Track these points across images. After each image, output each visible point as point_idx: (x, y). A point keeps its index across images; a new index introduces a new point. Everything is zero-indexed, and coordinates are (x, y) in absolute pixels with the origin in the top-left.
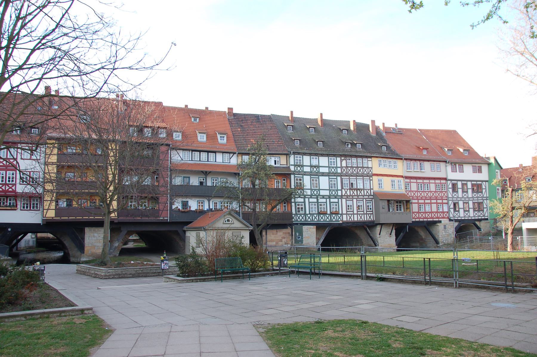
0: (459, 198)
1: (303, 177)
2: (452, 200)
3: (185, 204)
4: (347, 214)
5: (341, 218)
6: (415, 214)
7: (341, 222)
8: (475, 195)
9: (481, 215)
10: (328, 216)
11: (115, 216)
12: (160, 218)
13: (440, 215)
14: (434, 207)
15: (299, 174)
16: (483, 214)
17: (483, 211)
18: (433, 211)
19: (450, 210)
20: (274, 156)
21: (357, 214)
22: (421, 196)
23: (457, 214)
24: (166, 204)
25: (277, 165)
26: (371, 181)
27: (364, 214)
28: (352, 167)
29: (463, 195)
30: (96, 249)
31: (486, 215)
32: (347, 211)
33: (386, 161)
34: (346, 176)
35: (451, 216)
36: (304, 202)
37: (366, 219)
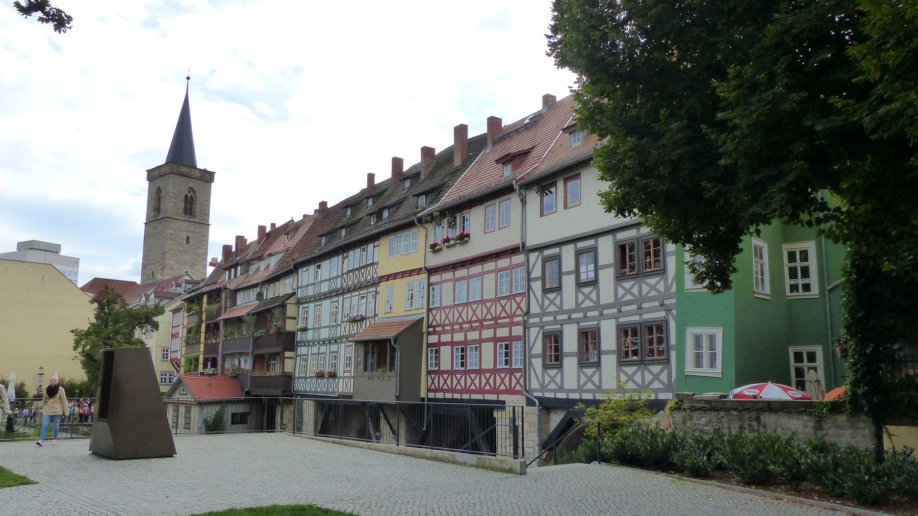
0: (565, 312)
1: (308, 307)
2: (541, 326)
4: (344, 377)
6: (445, 376)
8: (628, 291)
9: (656, 385)
10: (325, 380)
13: (503, 382)
14: (487, 357)
15: (306, 302)
16: (664, 377)
18: (483, 367)
19: (530, 363)
22: (460, 320)
23: (552, 379)
25: (291, 291)
26: (377, 295)
28: (354, 270)
29: (581, 297)
32: (345, 372)
33: (400, 236)
34: (349, 291)
35: (535, 384)
36: (307, 355)
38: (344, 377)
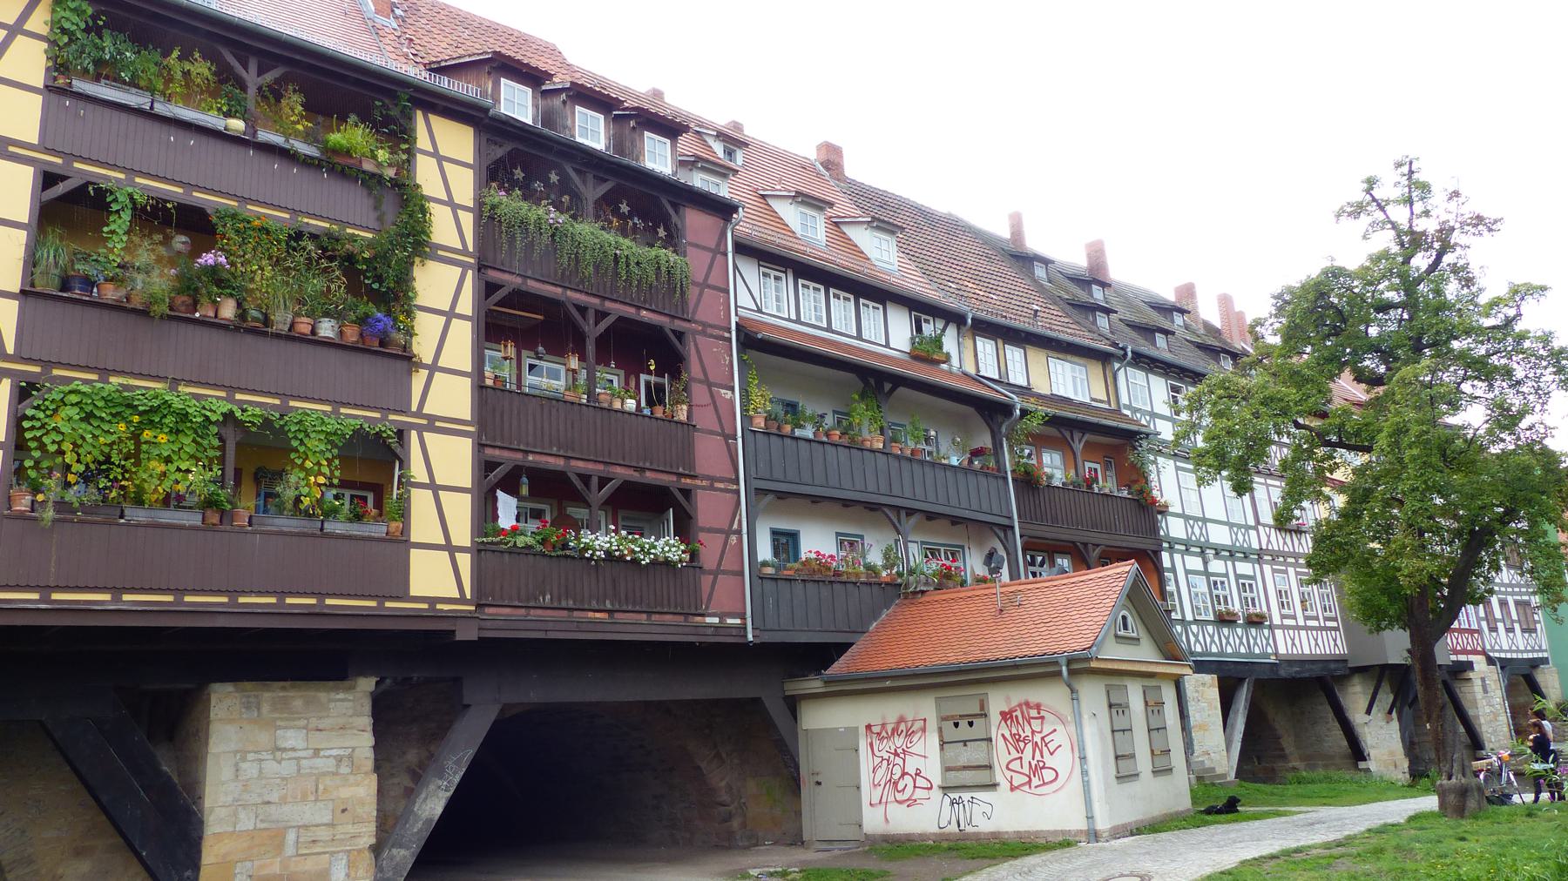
3: (786, 542)
4: (1283, 627)
5: (1271, 641)
7: (1272, 659)
10: (1239, 631)
11: (462, 600)
12: (709, 620)
17: (1535, 630)
20: (1069, 357)
21: (1306, 628)
24: (728, 533)
27: (1320, 629)
30: (290, 850)
31: (1544, 648)
32: (1283, 617)
37: (1328, 652)
38: (1283, 627)
